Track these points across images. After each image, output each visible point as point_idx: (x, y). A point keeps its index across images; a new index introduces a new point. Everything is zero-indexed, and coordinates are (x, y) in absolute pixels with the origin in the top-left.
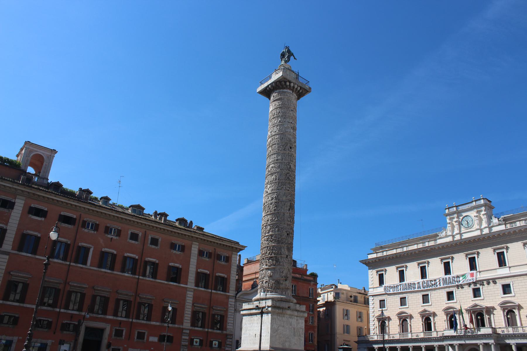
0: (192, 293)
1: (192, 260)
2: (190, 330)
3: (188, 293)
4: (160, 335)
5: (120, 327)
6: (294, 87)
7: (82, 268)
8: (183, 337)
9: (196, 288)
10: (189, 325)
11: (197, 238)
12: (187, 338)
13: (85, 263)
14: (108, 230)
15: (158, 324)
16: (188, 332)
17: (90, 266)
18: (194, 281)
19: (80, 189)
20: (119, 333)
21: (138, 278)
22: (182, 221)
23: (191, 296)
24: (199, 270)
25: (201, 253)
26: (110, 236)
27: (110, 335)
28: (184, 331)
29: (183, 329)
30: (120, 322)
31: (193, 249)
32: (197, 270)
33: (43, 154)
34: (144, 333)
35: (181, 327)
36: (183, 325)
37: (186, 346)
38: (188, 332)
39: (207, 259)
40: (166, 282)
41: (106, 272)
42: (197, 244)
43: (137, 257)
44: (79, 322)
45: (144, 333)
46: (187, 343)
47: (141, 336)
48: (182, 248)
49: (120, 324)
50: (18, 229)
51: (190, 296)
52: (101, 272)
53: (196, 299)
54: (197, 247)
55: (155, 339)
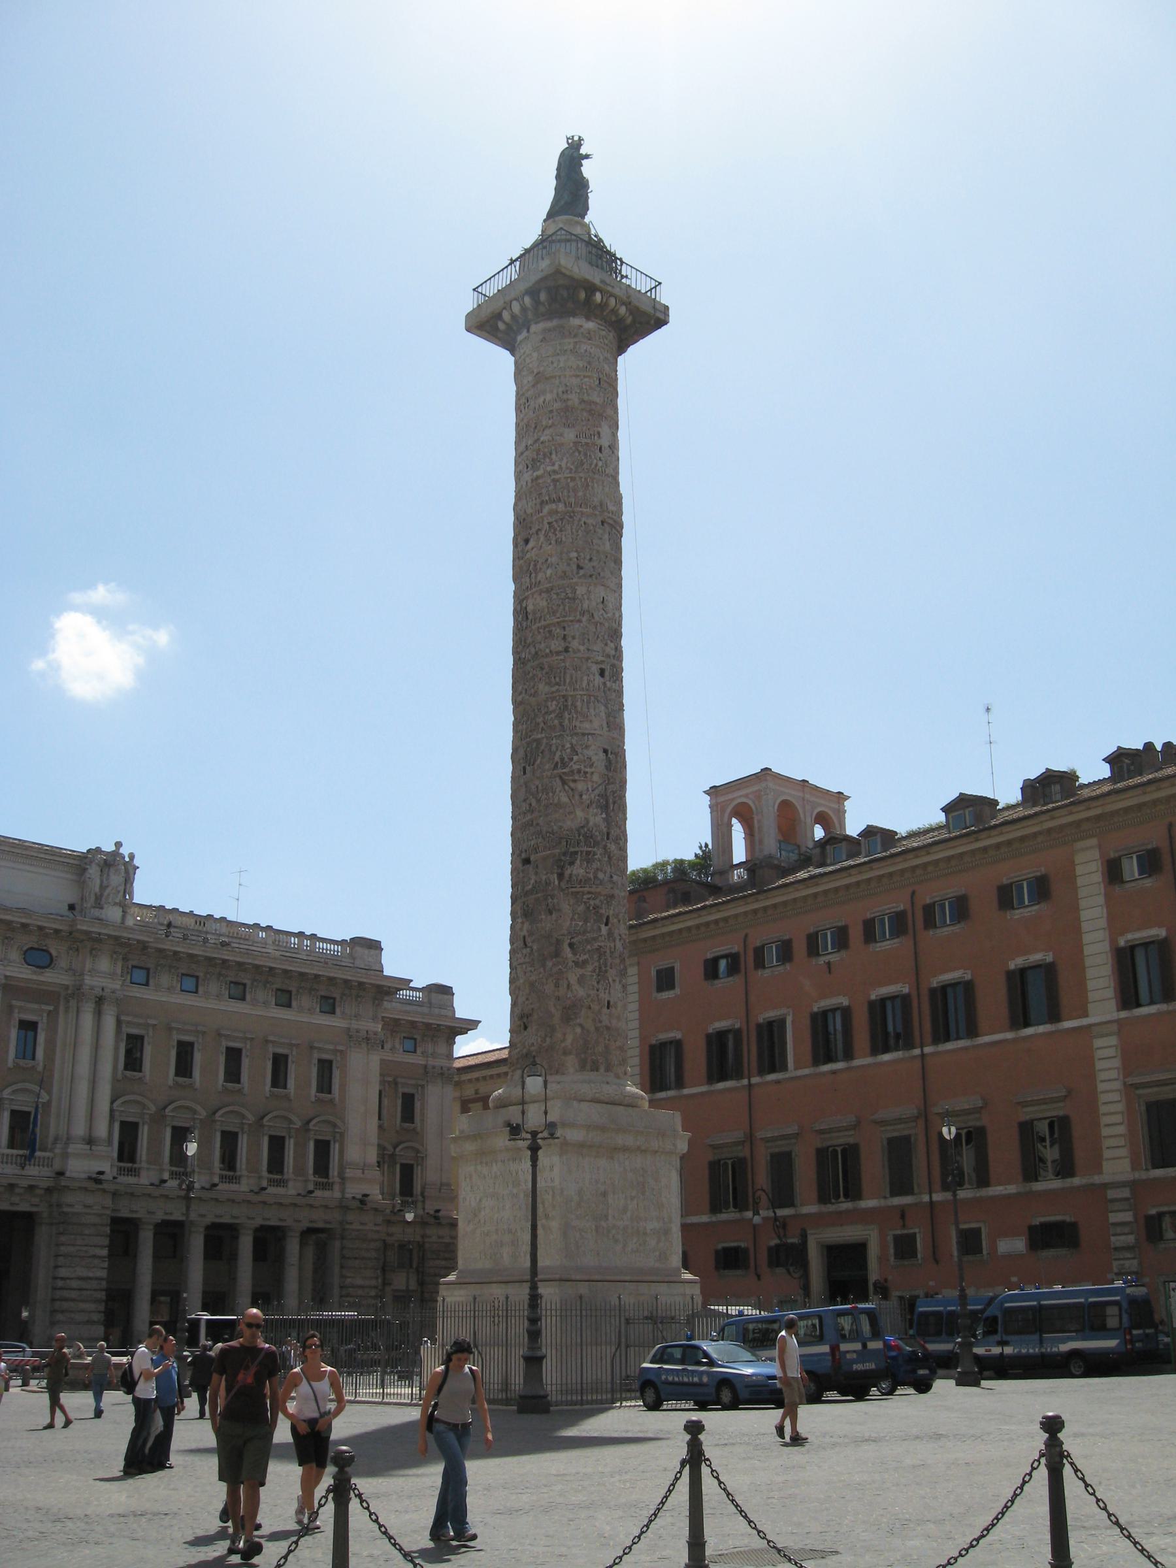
0: (1113, 1040)
1: (1085, 915)
2: (1133, 1185)
3: (1098, 1043)
4: (1032, 1229)
5: (904, 1226)
6: (513, 317)
7: (778, 1082)
8: (1114, 1218)
9: (1124, 1014)
10: (1126, 1164)
11: (1078, 824)
12: (1127, 1217)
13: (784, 1068)
14: (813, 946)
15: (1012, 1189)
16: (1126, 1193)
17: (796, 1069)
18: (1110, 993)
19: (947, 810)
20: (905, 1247)
21: (923, 1055)
22: (1120, 760)
23: (1111, 1052)
24: (1122, 943)
25: (1113, 872)
26: (822, 960)
27: (882, 1259)
28: (1111, 1194)
29: (1105, 1186)
30: (903, 1213)
31: (1079, 870)
32: (1113, 941)
33: (746, 796)
34: (979, 1230)
35: (1097, 1179)
36: (1100, 1173)
37: (1128, 1248)
38: (1126, 1193)
39: (1148, 883)
40: (1009, 1035)
41: (834, 1072)
42: (1094, 841)
43: (906, 990)
44: (804, 1236)
45: (979, 1230)
46: (1131, 1239)
47: (970, 1242)
48: (1042, 888)
49: (903, 1216)
50: (642, 1039)
52: (824, 1074)
53: (1130, 1059)
54: (1096, 854)
55: (1019, 1245)
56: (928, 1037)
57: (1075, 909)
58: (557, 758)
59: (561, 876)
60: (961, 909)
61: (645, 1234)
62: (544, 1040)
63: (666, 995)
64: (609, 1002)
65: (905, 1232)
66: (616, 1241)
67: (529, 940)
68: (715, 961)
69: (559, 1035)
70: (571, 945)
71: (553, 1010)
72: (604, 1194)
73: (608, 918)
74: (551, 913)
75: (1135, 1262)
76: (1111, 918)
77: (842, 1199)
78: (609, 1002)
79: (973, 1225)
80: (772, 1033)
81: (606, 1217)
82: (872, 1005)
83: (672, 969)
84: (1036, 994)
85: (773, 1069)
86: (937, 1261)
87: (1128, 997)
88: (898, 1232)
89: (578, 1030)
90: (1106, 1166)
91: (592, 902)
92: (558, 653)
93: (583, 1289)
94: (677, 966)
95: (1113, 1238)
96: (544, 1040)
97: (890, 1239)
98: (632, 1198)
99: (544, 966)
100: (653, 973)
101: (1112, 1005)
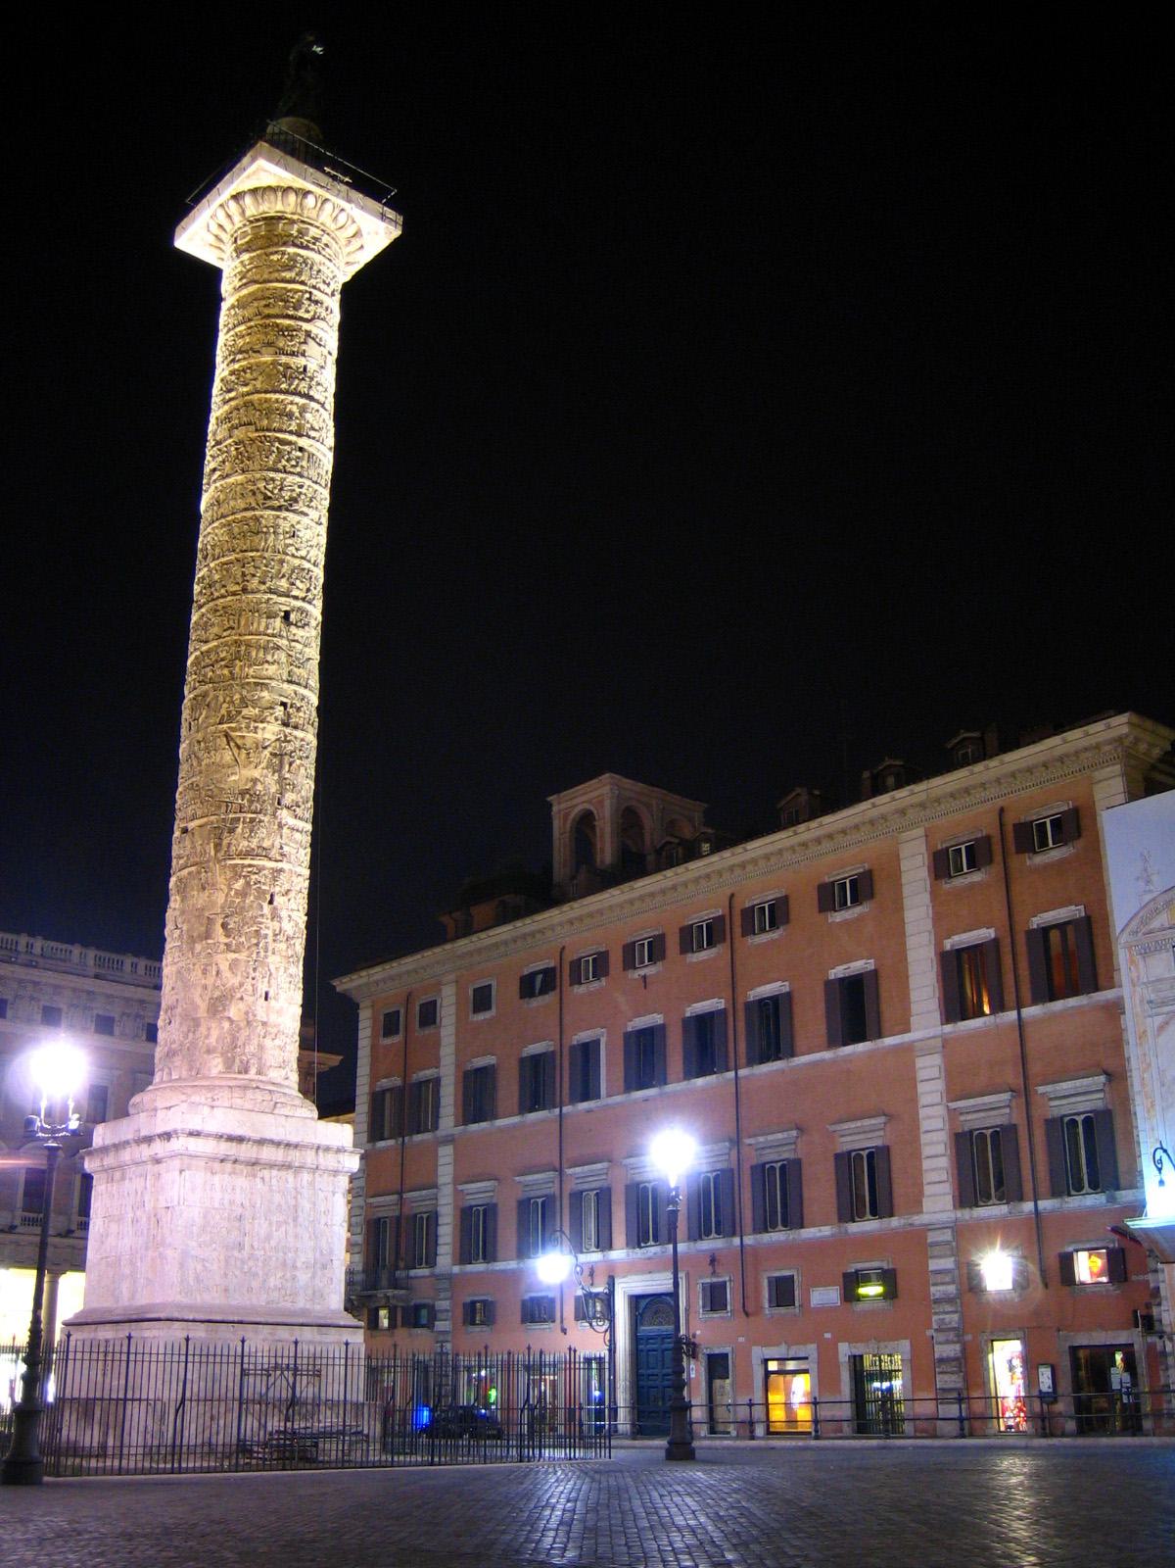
7: (589, 1111)
8: (934, 1265)
13: (598, 1096)
15: (826, 1231)
16: (947, 1236)
17: (609, 1095)
23: (935, 1072)
24: (948, 945)
28: (932, 1237)
29: (928, 1228)
32: (938, 943)
33: (589, 801)
35: (917, 1220)
37: (949, 1300)
38: (947, 1236)
40: (827, 1055)
46: (951, 1289)
51: (930, 1072)
56: (743, 1060)
57: (899, 908)
58: (223, 711)
59: (218, 847)
60: (777, 913)
61: (294, 1267)
62: (186, 1036)
63: (481, 1017)
64: (267, 994)
65: (715, 1280)
66: (255, 1275)
67: (180, 920)
68: (533, 975)
69: (203, 1030)
70: (224, 926)
71: (198, 1000)
72: (240, 1218)
73: (272, 896)
74: (204, 889)
75: (956, 1317)
76: (937, 919)
77: (651, 1243)
78: (267, 994)
79: (787, 1273)
80: (588, 1052)
81: (240, 1246)
82: (686, 1022)
83: (489, 986)
84: (857, 1009)
85: (586, 1097)
86: (747, 1314)
87: (956, 1007)
88: (708, 1280)
89: (226, 1025)
90: (927, 1204)
91: (254, 877)
92: (234, 594)
93: (199, 1333)
94: (494, 984)
95: (933, 1289)
96: (186, 1036)
97: (699, 1288)
98: (279, 1224)
99: (192, 949)
100: (471, 993)
101: (937, 1016)
